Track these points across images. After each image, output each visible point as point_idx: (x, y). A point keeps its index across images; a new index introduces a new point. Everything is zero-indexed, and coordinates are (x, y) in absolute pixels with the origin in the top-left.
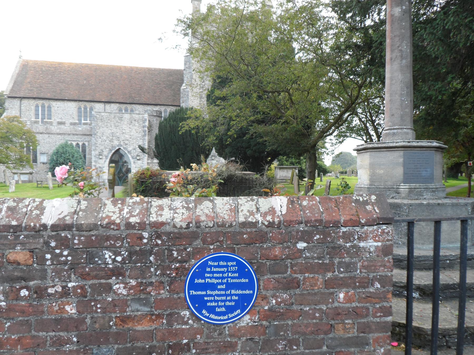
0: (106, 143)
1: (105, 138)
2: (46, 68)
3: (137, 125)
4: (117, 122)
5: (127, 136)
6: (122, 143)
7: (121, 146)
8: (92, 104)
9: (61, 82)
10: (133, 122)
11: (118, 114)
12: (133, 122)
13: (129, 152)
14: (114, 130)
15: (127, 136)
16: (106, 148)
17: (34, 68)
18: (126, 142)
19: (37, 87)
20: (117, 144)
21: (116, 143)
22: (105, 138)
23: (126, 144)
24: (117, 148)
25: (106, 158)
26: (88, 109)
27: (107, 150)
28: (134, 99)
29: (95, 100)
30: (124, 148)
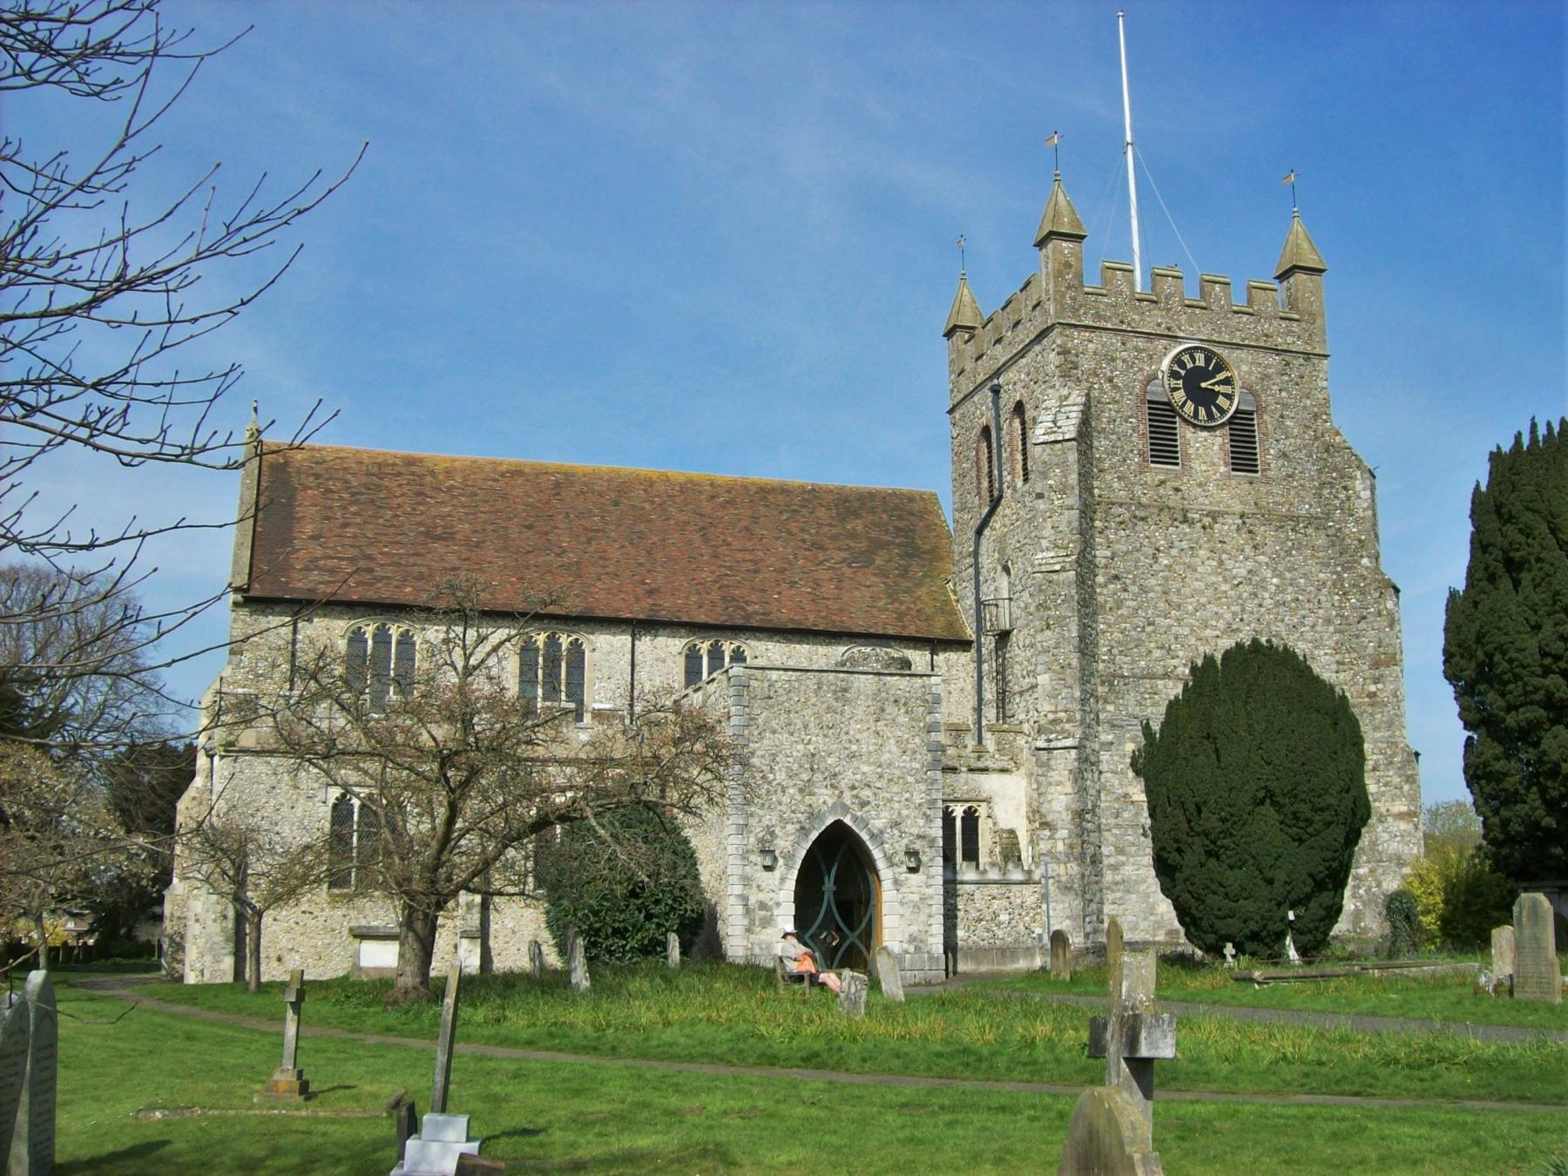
0: (786, 799)
1: (781, 776)
2: (364, 479)
3: (903, 719)
4: (829, 709)
5: (865, 768)
6: (847, 798)
7: (846, 809)
9: (438, 538)
10: (890, 709)
11: (831, 676)
12: (890, 709)
13: (873, 836)
14: (819, 742)
15: (865, 768)
16: (784, 822)
17: (317, 476)
18: (866, 793)
19: (352, 560)
20: (830, 802)
21: (824, 797)
22: (781, 776)
23: (864, 804)
24: (829, 821)
25: (789, 867)
27: (790, 827)
28: (743, 609)
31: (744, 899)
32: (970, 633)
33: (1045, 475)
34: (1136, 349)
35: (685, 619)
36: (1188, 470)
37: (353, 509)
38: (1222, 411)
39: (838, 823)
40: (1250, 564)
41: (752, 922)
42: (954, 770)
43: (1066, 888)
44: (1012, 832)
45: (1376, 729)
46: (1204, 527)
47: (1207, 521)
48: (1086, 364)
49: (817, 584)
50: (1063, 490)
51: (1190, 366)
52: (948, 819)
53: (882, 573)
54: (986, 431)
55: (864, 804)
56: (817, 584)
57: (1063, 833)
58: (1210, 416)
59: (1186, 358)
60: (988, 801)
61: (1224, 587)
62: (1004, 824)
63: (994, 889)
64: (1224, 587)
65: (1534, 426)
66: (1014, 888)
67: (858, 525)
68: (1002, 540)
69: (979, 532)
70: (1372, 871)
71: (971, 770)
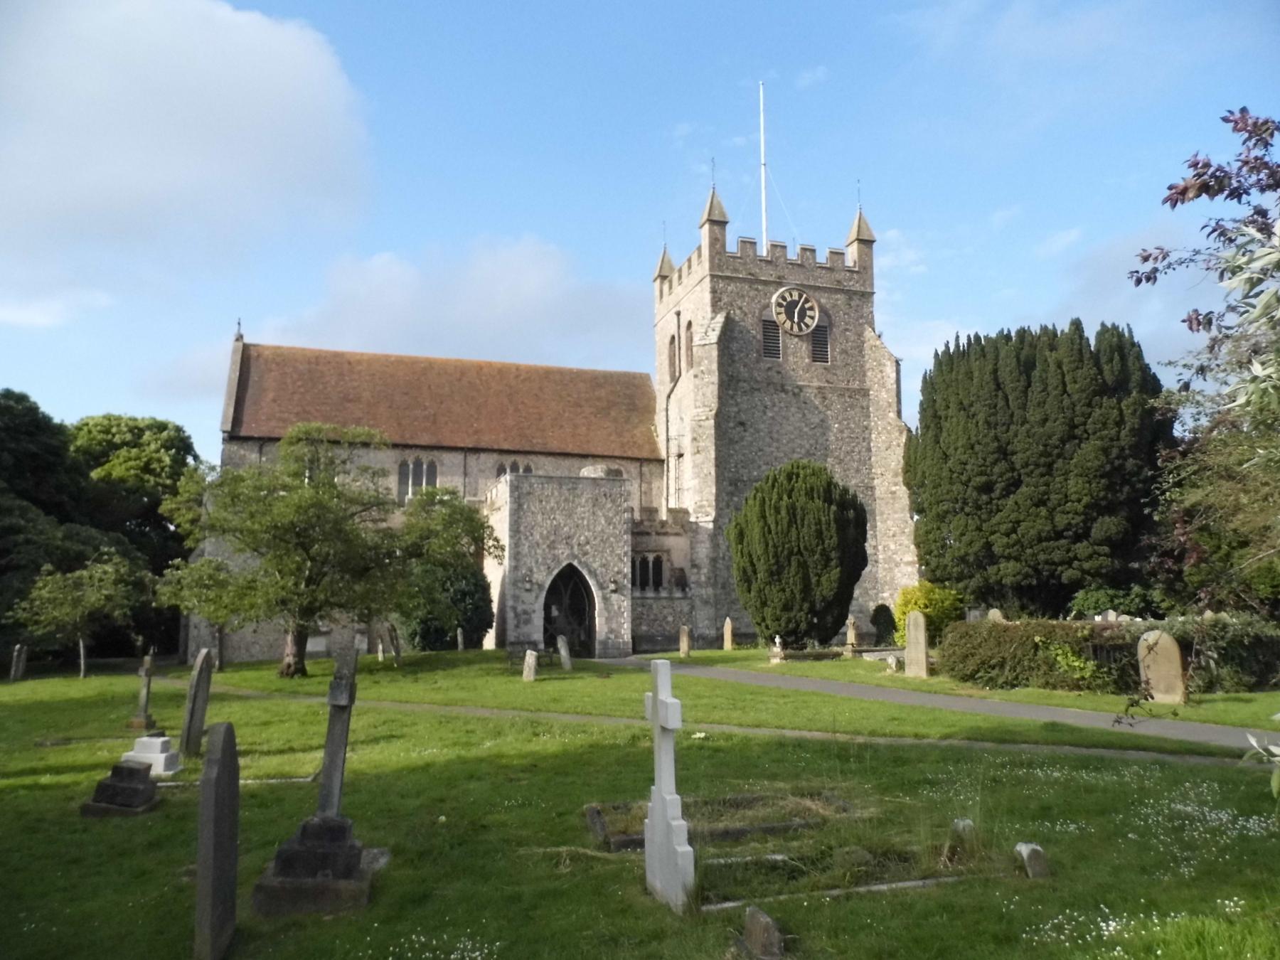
0: (539, 551)
7: (575, 557)
8: (436, 453)
13: (590, 572)
17: (278, 364)
23: (586, 554)
24: (564, 564)
26: (425, 467)
29: (445, 444)
30: (580, 562)
31: (514, 609)
32: (663, 455)
33: (699, 364)
34: (757, 289)
35: (496, 447)
36: (786, 360)
37: (299, 383)
38: (807, 326)
39: (570, 566)
40: (822, 416)
41: (519, 622)
42: (648, 534)
43: (706, 602)
44: (682, 570)
45: (896, 512)
46: (794, 394)
47: (796, 391)
48: (725, 299)
49: (576, 426)
50: (710, 372)
51: (789, 299)
52: (644, 562)
53: (615, 420)
54: (673, 338)
55: (586, 554)
56: (576, 426)
57: (705, 571)
58: (800, 329)
59: (787, 295)
60: (668, 551)
61: (806, 429)
62: (677, 565)
63: (665, 603)
64: (806, 429)
65: (957, 337)
66: (677, 603)
67: (602, 393)
68: (680, 401)
69: (669, 397)
70: (892, 595)
71: (658, 534)
